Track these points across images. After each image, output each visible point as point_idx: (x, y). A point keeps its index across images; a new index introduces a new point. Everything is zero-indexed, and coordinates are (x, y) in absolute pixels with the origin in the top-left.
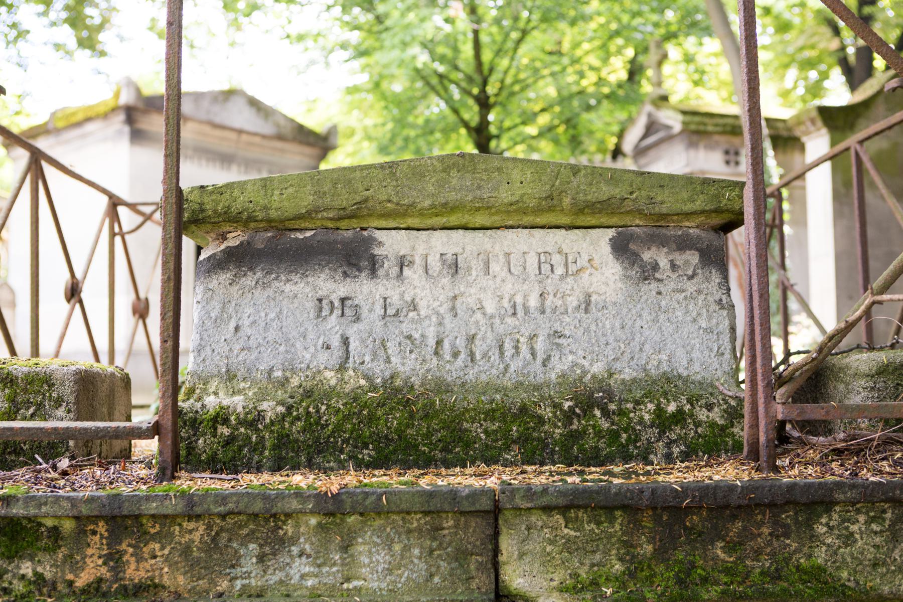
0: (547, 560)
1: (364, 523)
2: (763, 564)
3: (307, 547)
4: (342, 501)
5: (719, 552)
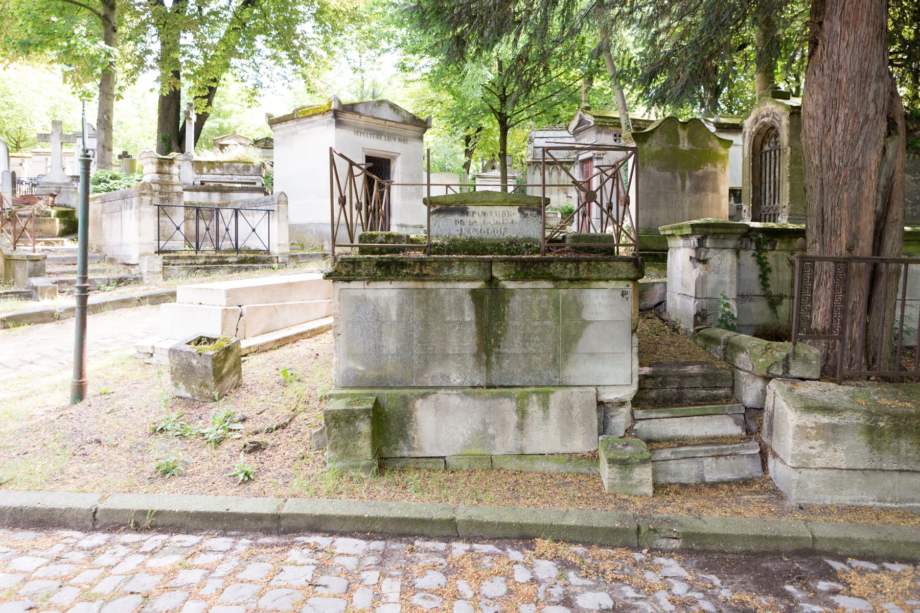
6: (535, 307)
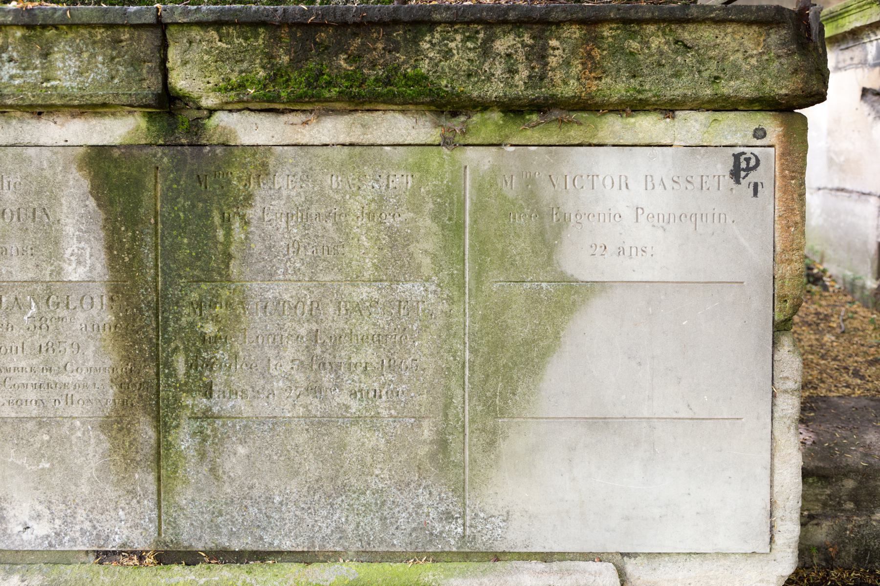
0: (204, 67)
1: (59, 36)
2: (378, 73)
3: (15, 54)
4: (35, 15)
5: (342, 62)
6: (358, 226)
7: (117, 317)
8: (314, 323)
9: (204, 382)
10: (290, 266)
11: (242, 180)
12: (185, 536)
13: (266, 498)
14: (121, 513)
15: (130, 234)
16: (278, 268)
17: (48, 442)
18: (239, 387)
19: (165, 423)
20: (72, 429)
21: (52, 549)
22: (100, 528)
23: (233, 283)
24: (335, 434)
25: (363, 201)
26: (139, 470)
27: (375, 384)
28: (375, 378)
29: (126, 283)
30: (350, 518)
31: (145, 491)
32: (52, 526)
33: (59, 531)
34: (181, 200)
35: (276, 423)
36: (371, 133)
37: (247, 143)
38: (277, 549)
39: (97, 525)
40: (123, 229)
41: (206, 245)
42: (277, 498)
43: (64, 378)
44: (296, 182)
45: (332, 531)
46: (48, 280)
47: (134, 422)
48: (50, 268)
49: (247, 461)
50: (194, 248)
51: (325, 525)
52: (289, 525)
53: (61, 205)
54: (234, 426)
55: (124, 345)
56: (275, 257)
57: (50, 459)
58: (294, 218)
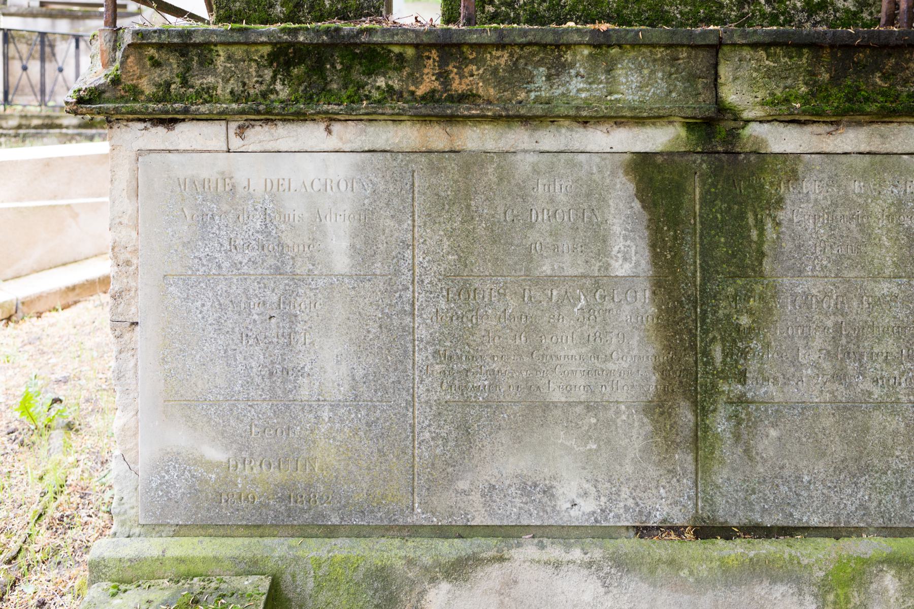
0: (753, 82)
1: (622, 54)
2: (909, 90)
3: (581, 70)
4: (610, 35)
5: (877, 80)
6: (880, 226)
7: (659, 308)
8: (840, 316)
9: (739, 370)
10: (818, 264)
11: (774, 185)
12: (721, 513)
13: (796, 477)
14: (662, 491)
15: (672, 233)
16: (807, 266)
17: (595, 425)
18: (771, 374)
19: (703, 408)
20: (618, 413)
21: (598, 524)
22: (642, 505)
23: (765, 278)
24: (859, 418)
25: (884, 205)
26: (679, 451)
27: (896, 372)
28: (895, 367)
29: (668, 279)
30: (873, 496)
31: (685, 471)
32: (598, 503)
33: (604, 507)
34: (718, 202)
35: (805, 408)
36: (890, 143)
37: (777, 151)
38: (806, 525)
39: (640, 502)
40: (665, 228)
41: (741, 244)
42: (806, 477)
43: (611, 366)
44: (823, 187)
45: (856, 508)
46: (596, 275)
47: (674, 407)
48: (598, 264)
49: (778, 443)
50: (731, 247)
51: (849, 503)
52: (817, 502)
53: (609, 206)
54: (766, 410)
55: (666, 336)
56: (804, 255)
57: (597, 440)
58: (821, 220)
